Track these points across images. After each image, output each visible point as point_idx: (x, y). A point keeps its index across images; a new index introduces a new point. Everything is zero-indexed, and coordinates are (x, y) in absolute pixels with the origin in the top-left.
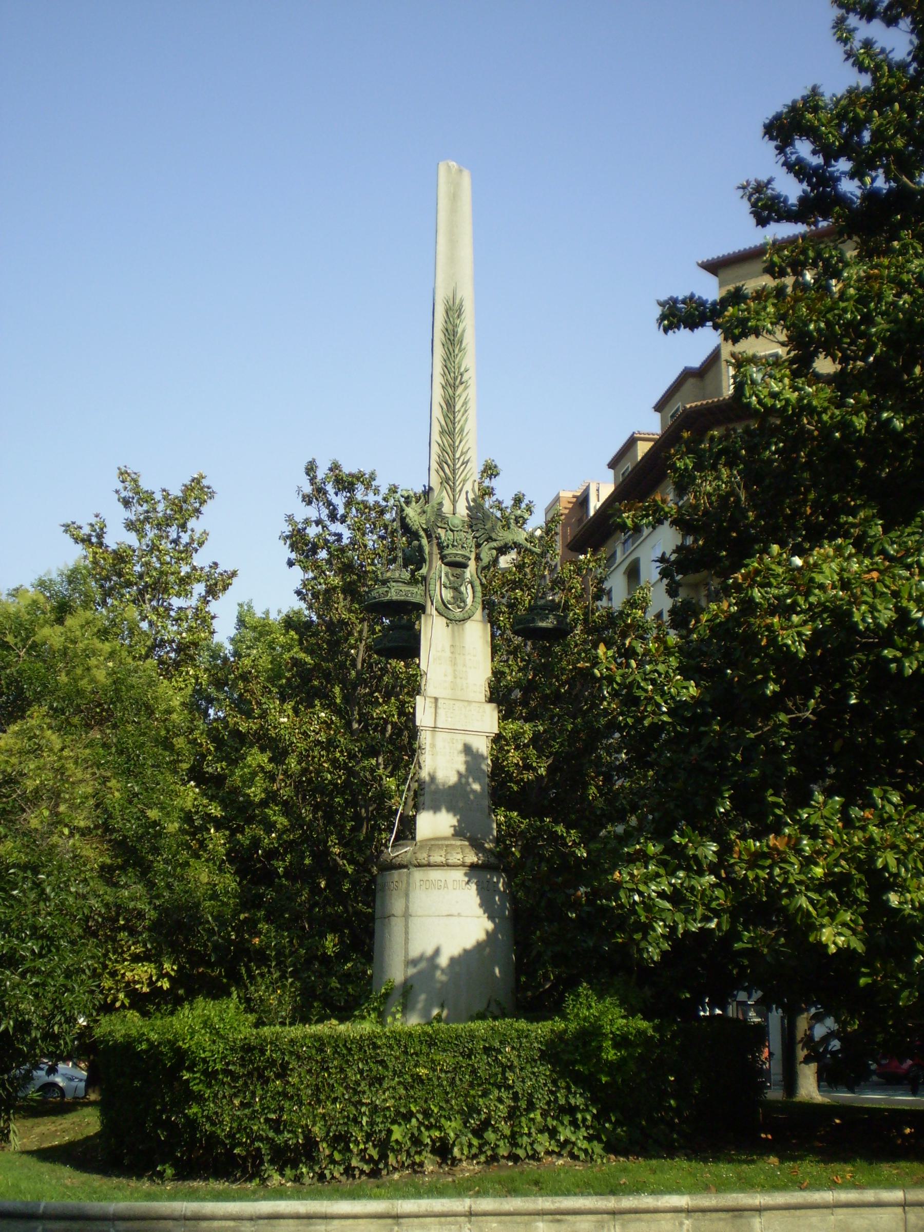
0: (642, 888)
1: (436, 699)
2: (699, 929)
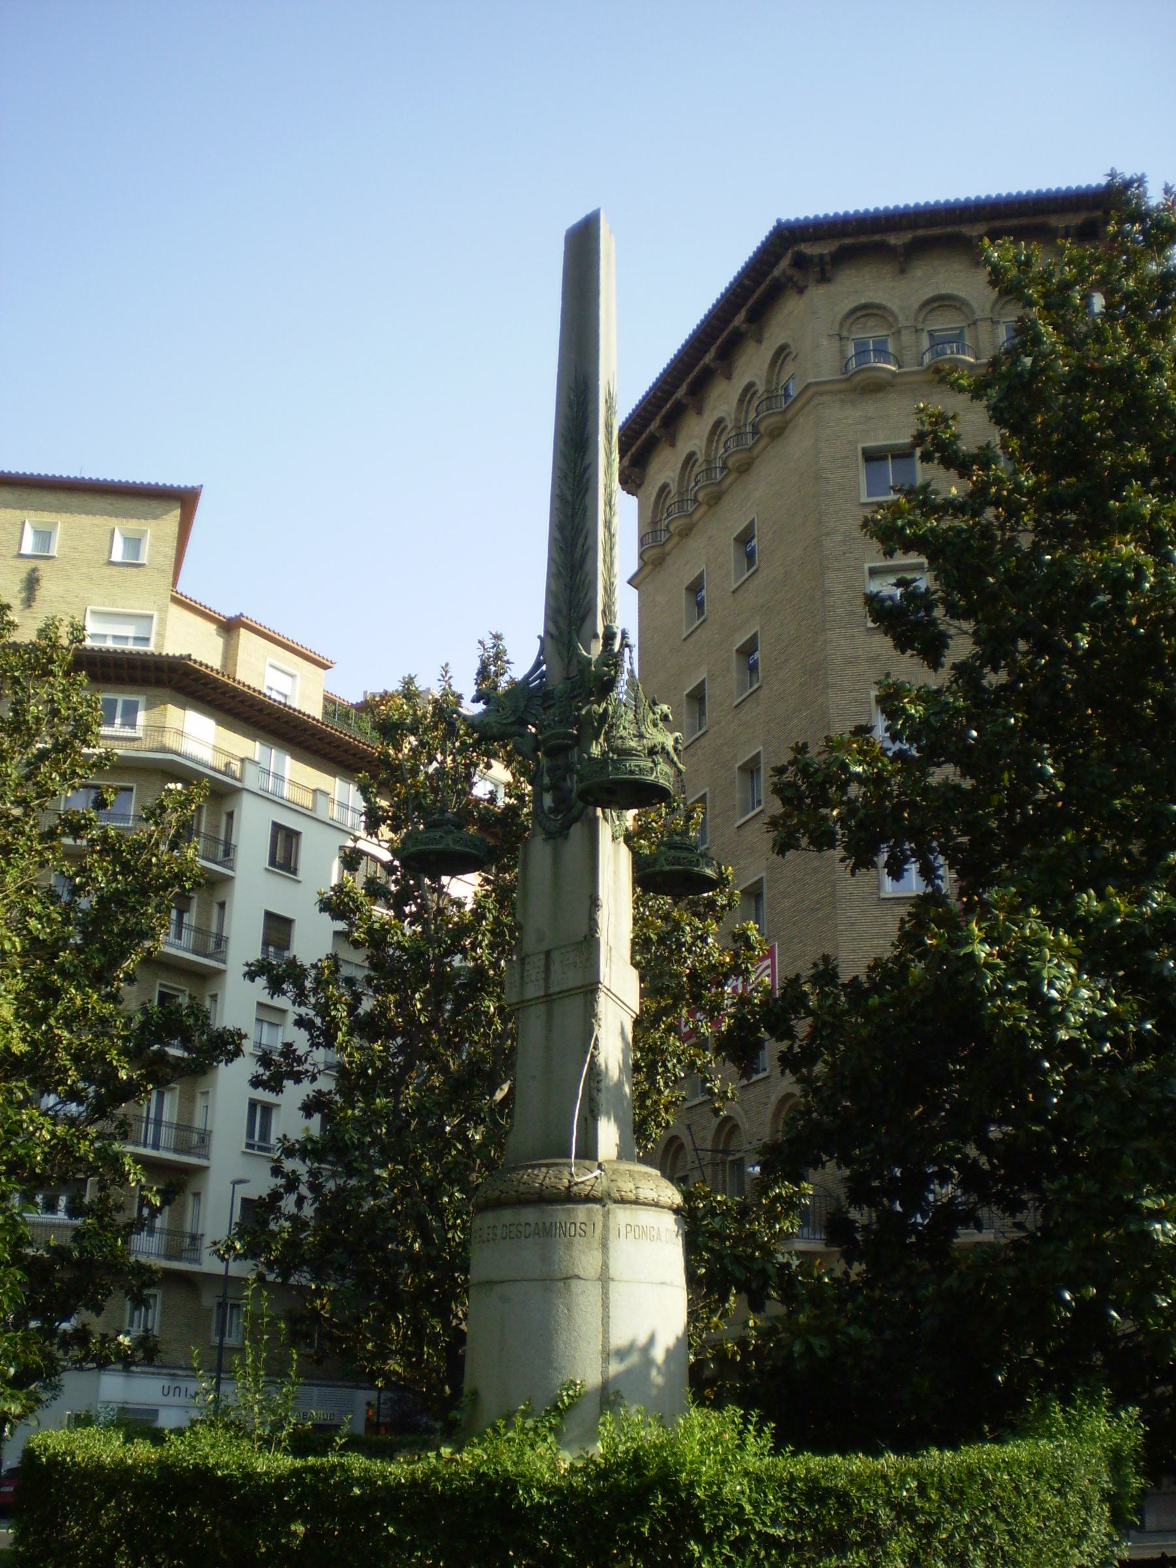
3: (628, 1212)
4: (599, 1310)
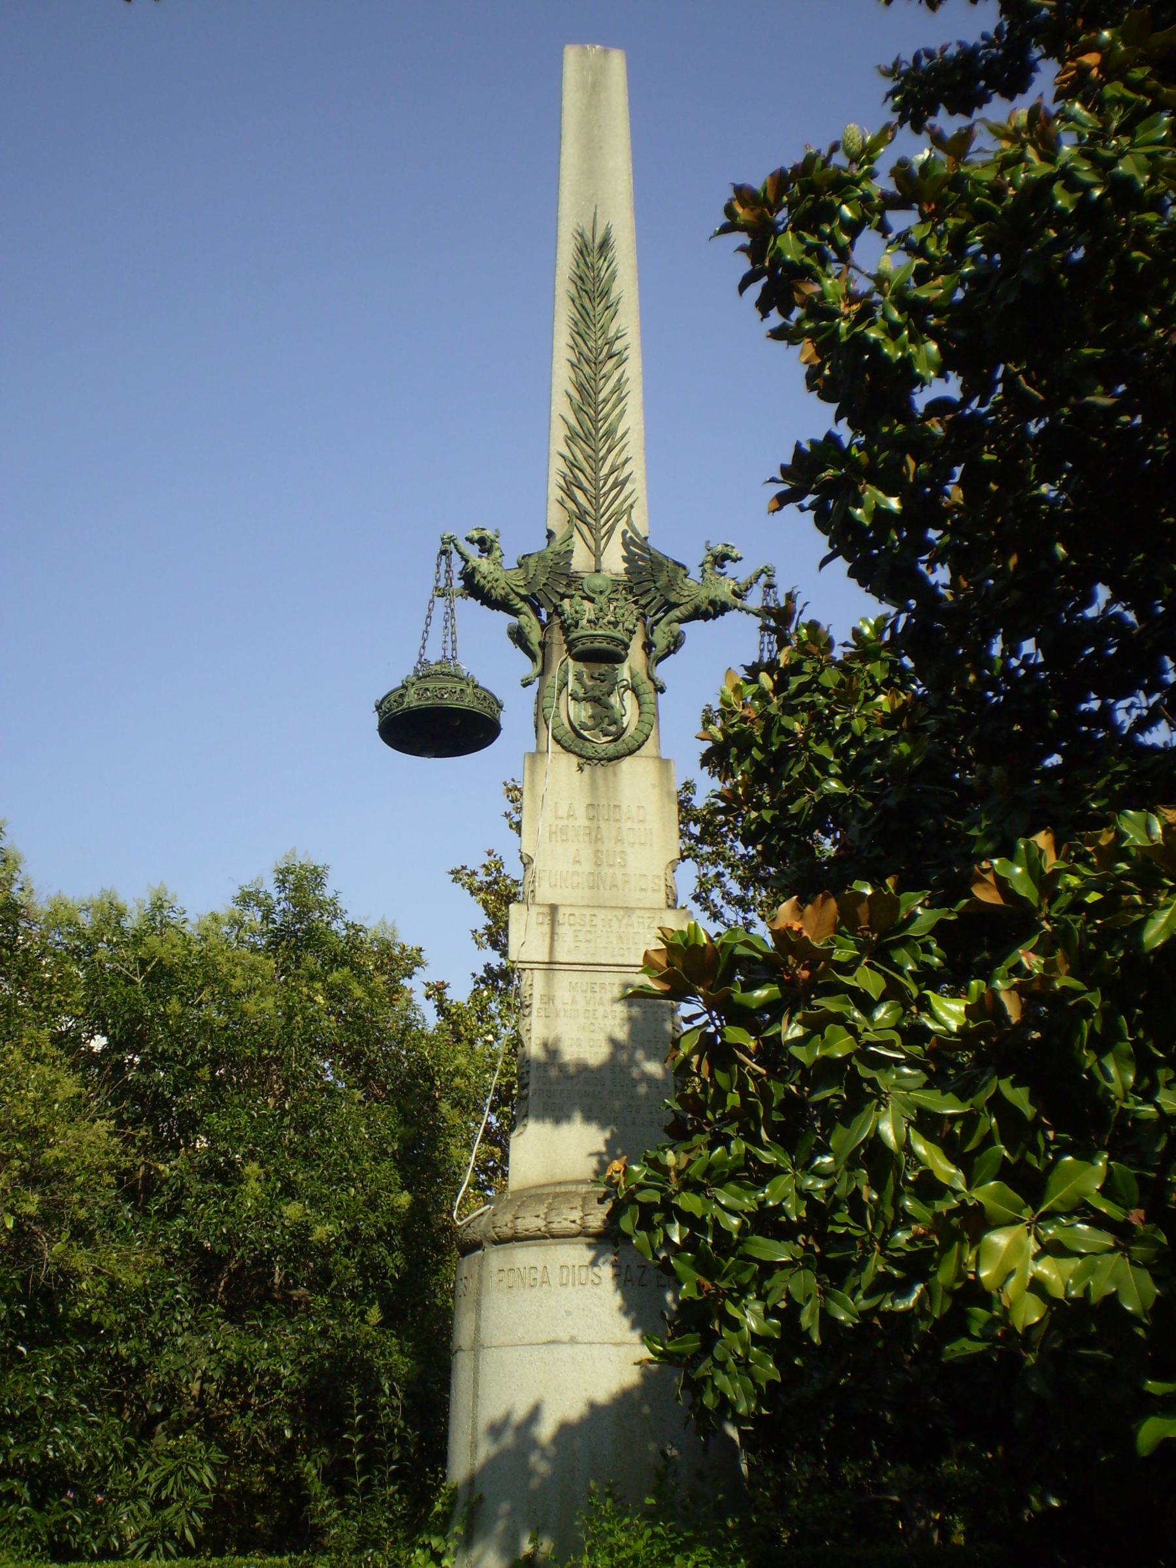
0: (688, 1202)
1: (554, 908)
2: (864, 1315)
3: (501, 1254)
4: (471, 1392)
